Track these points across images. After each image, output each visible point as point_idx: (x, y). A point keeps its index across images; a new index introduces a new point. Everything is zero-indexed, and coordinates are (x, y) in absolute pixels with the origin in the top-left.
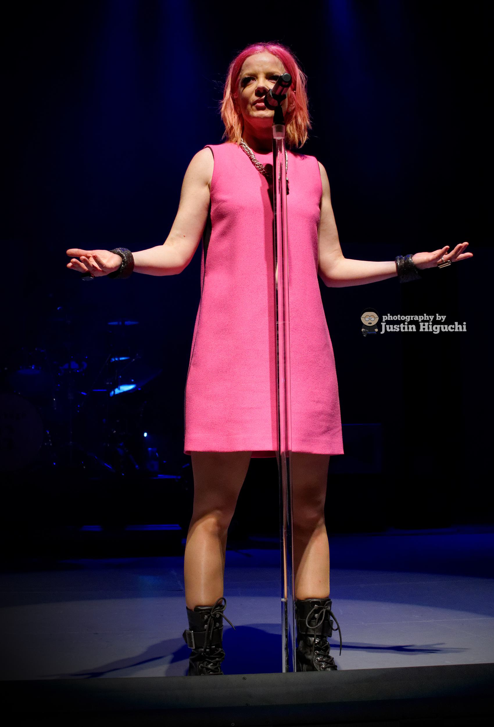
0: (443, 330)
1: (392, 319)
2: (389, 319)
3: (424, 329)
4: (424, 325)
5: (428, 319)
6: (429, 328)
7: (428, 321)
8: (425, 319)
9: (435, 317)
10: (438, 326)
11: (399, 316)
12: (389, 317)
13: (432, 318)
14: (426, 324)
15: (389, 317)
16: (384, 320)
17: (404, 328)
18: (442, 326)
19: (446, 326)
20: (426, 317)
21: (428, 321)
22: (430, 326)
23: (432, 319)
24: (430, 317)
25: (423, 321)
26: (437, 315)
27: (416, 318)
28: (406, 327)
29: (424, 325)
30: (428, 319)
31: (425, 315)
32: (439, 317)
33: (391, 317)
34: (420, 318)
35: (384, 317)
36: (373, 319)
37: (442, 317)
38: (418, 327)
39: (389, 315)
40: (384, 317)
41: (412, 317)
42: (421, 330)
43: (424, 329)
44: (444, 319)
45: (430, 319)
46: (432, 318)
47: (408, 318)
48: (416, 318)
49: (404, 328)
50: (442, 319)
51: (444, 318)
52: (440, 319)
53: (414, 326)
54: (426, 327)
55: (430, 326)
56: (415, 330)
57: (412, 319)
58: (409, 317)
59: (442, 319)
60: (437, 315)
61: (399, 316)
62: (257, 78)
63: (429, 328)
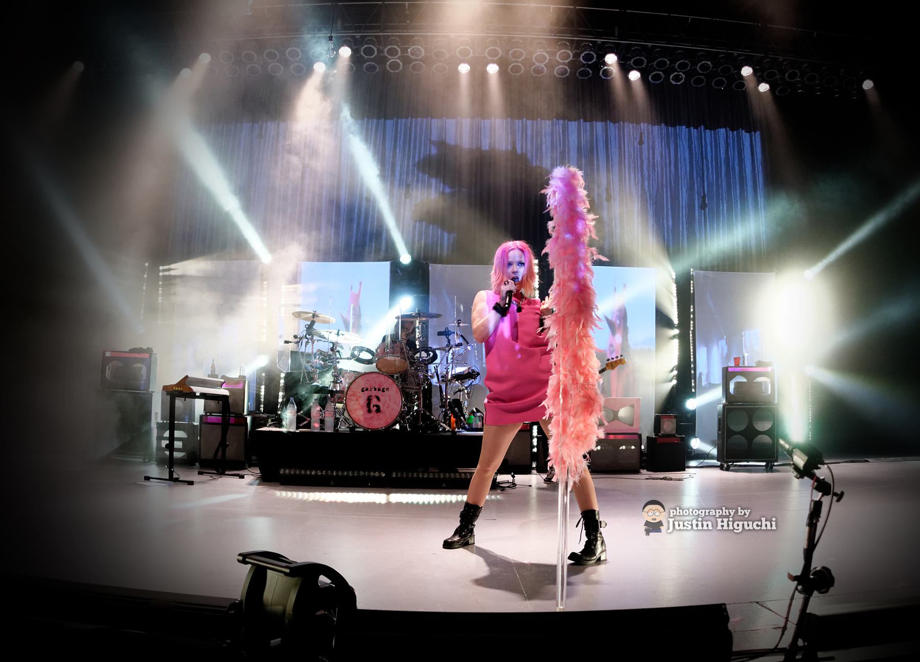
0: (746, 527)
3: (722, 526)
4: (722, 522)
6: (728, 526)
7: (728, 517)
9: (737, 511)
10: (741, 523)
14: (726, 520)
16: (672, 515)
17: (697, 525)
18: (746, 523)
19: (750, 523)
20: (725, 512)
21: (728, 517)
22: (731, 523)
25: (720, 517)
28: (700, 523)
29: (722, 522)
32: (741, 512)
36: (658, 514)
38: (715, 525)
42: (719, 527)
43: (722, 526)
49: (697, 525)
53: (710, 523)
54: (725, 524)
55: (731, 523)
56: (710, 527)
62: (335, 204)
63: (728, 526)
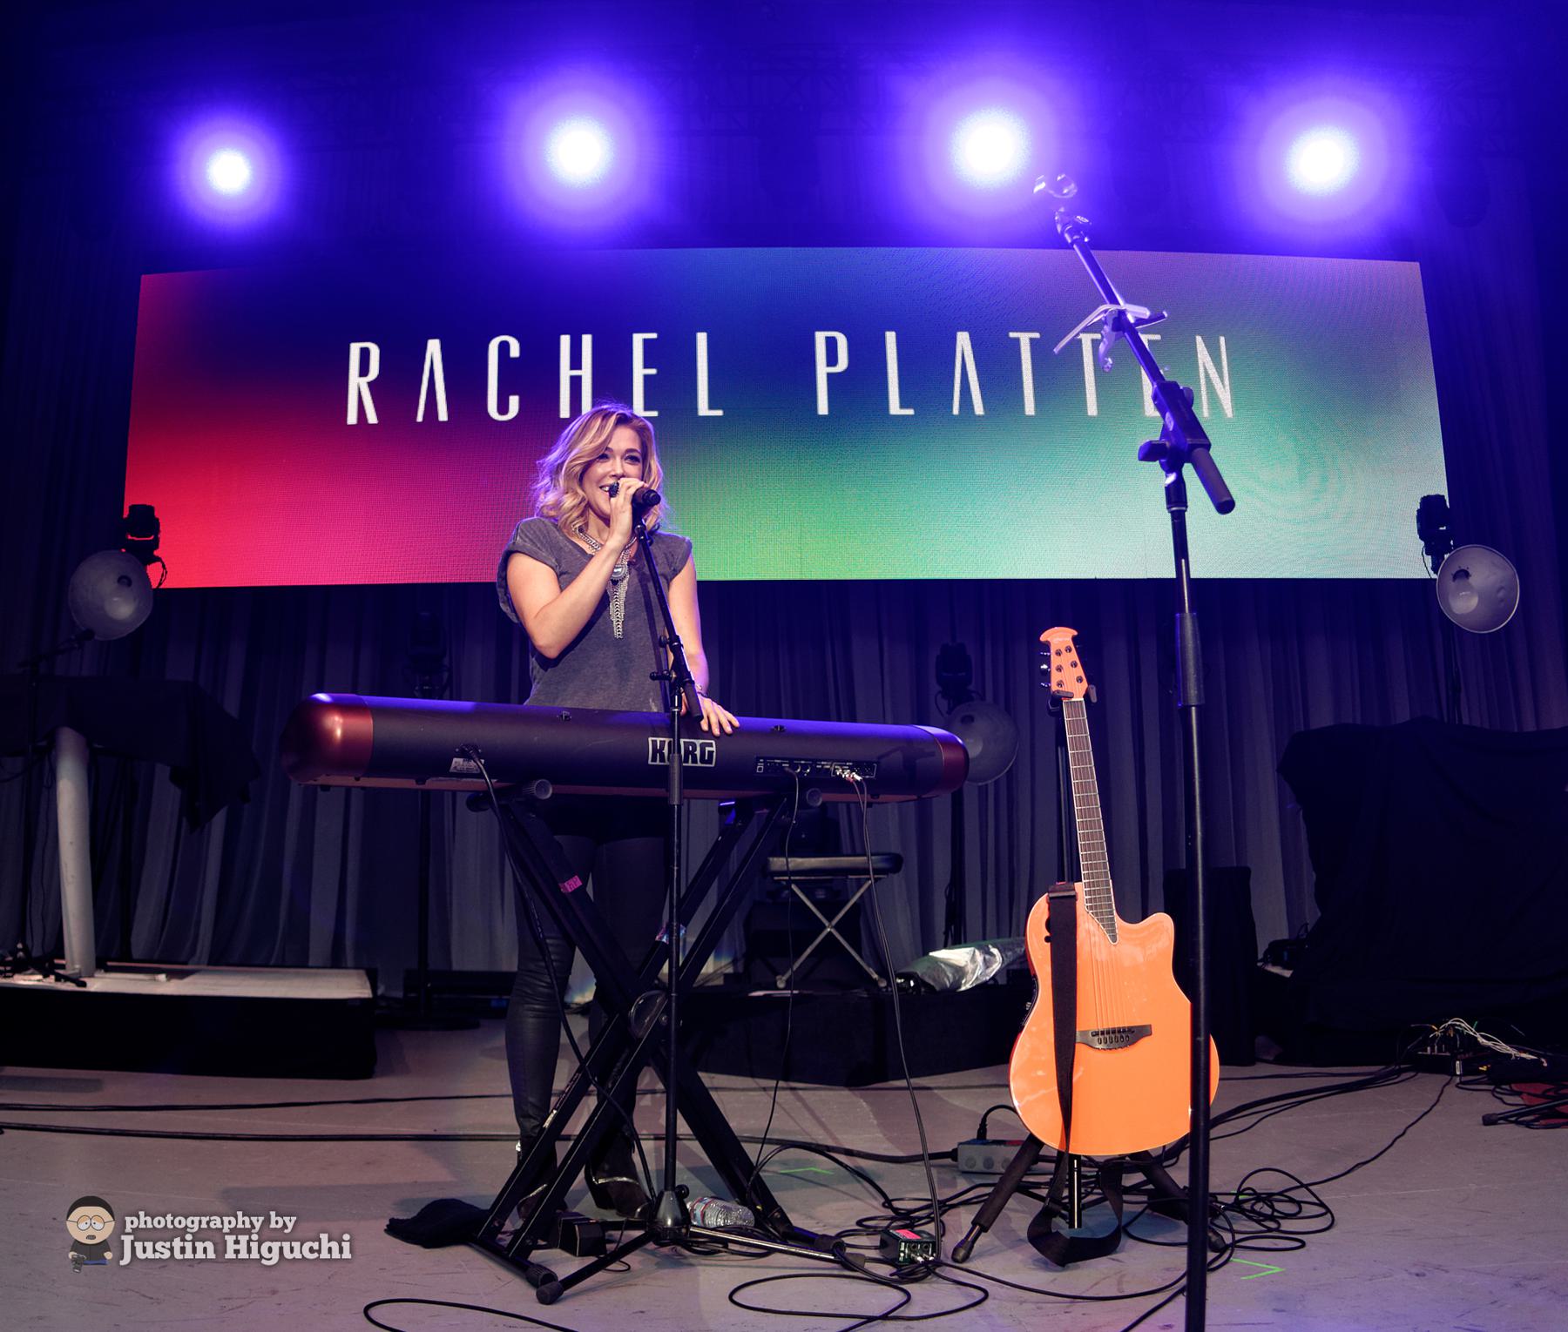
1: (150, 1226)
2: (142, 1226)
5: (248, 1226)
8: (240, 1226)
9: (267, 1220)
11: (169, 1217)
12: (144, 1221)
13: (258, 1222)
15: (144, 1221)
16: (128, 1228)
20: (242, 1221)
23: (258, 1226)
24: (254, 1219)
26: (273, 1214)
27: (216, 1222)
30: (248, 1226)
31: (240, 1214)
32: (276, 1221)
33: (149, 1219)
34: (228, 1223)
35: (128, 1219)
37: (287, 1219)
39: (142, 1214)
40: (128, 1219)
41: (205, 1220)
44: (290, 1226)
45: (253, 1226)
46: (258, 1222)
47: (193, 1224)
48: (216, 1222)
50: (285, 1226)
51: (290, 1222)
52: (280, 1225)
57: (204, 1226)
58: (196, 1219)
59: (285, 1226)
60: (273, 1214)
61: (169, 1217)
